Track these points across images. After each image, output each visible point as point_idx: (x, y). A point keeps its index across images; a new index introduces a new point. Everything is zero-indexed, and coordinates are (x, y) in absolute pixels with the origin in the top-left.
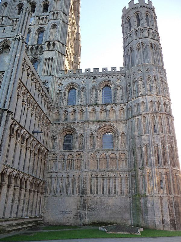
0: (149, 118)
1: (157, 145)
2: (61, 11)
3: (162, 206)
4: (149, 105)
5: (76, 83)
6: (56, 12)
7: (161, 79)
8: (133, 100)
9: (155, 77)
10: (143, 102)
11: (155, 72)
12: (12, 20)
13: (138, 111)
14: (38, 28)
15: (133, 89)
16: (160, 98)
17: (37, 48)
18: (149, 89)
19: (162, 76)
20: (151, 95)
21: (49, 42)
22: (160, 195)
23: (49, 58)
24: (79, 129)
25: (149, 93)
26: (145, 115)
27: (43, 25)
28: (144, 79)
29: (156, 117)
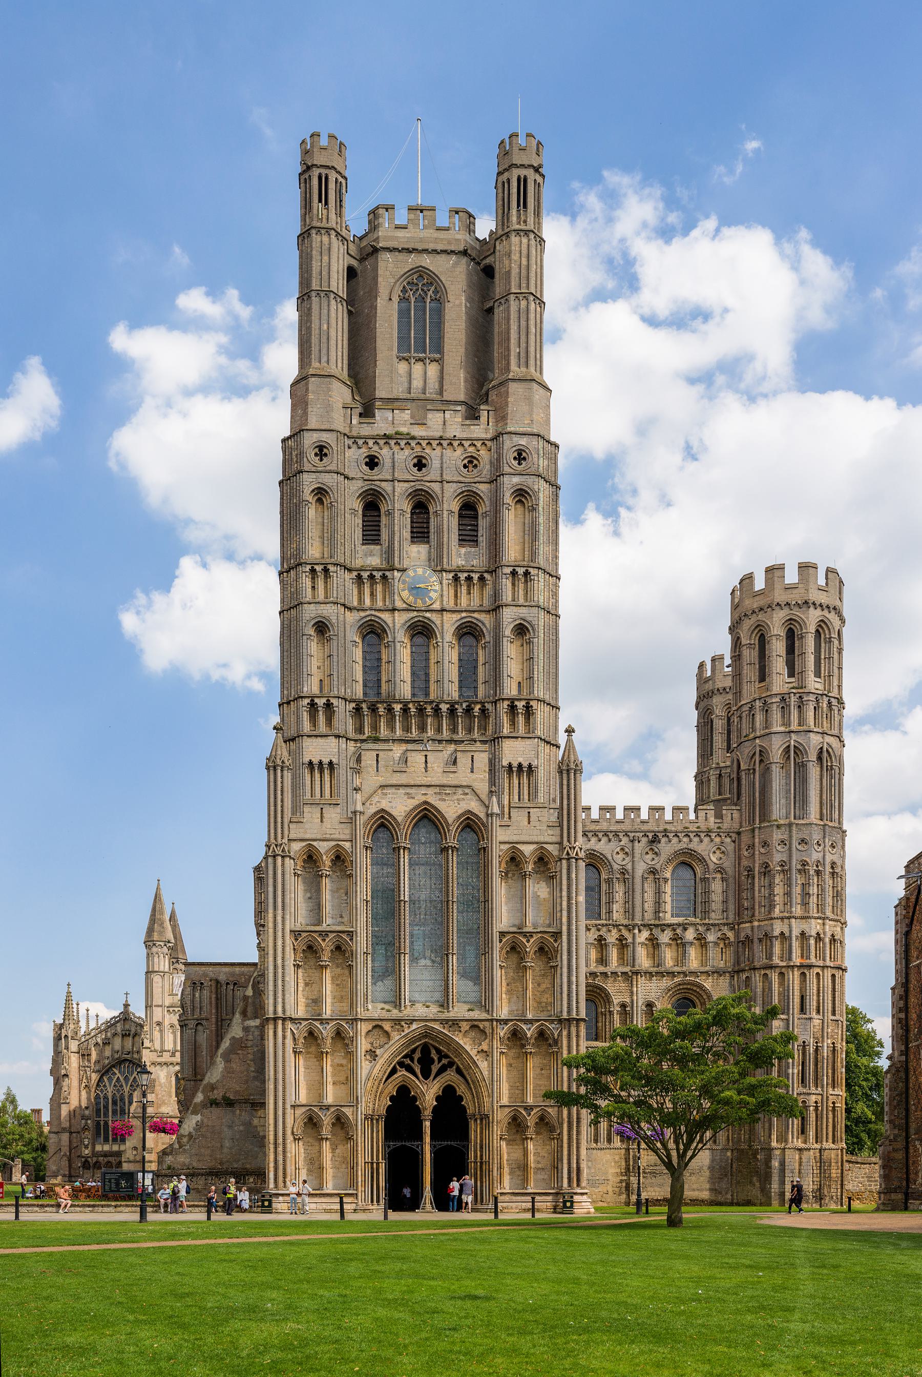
0: (794, 977)
1: (804, 1042)
2: (539, 568)
3: (800, 1165)
4: (795, 944)
5: (602, 854)
6: (521, 571)
7: (832, 868)
8: (756, 924)
9: (817, 866)
10: (782, 934)
11: (821, 848)
12: (355, 573)
13: (770, 956)
14: (459, 623)
15: (760, 891)
16: (824, 924)
17: (468, 711)
18: (799, 901)
19: (835, 858)
20: (802, 918)
21: (512, 700)
22: (800, 1145)
23: (520, 766)
24: (617, 992)
25: (797, 910)
26: (783, 970)
27: (476, 615)
28: (790, 869)
29: (808, 976)
